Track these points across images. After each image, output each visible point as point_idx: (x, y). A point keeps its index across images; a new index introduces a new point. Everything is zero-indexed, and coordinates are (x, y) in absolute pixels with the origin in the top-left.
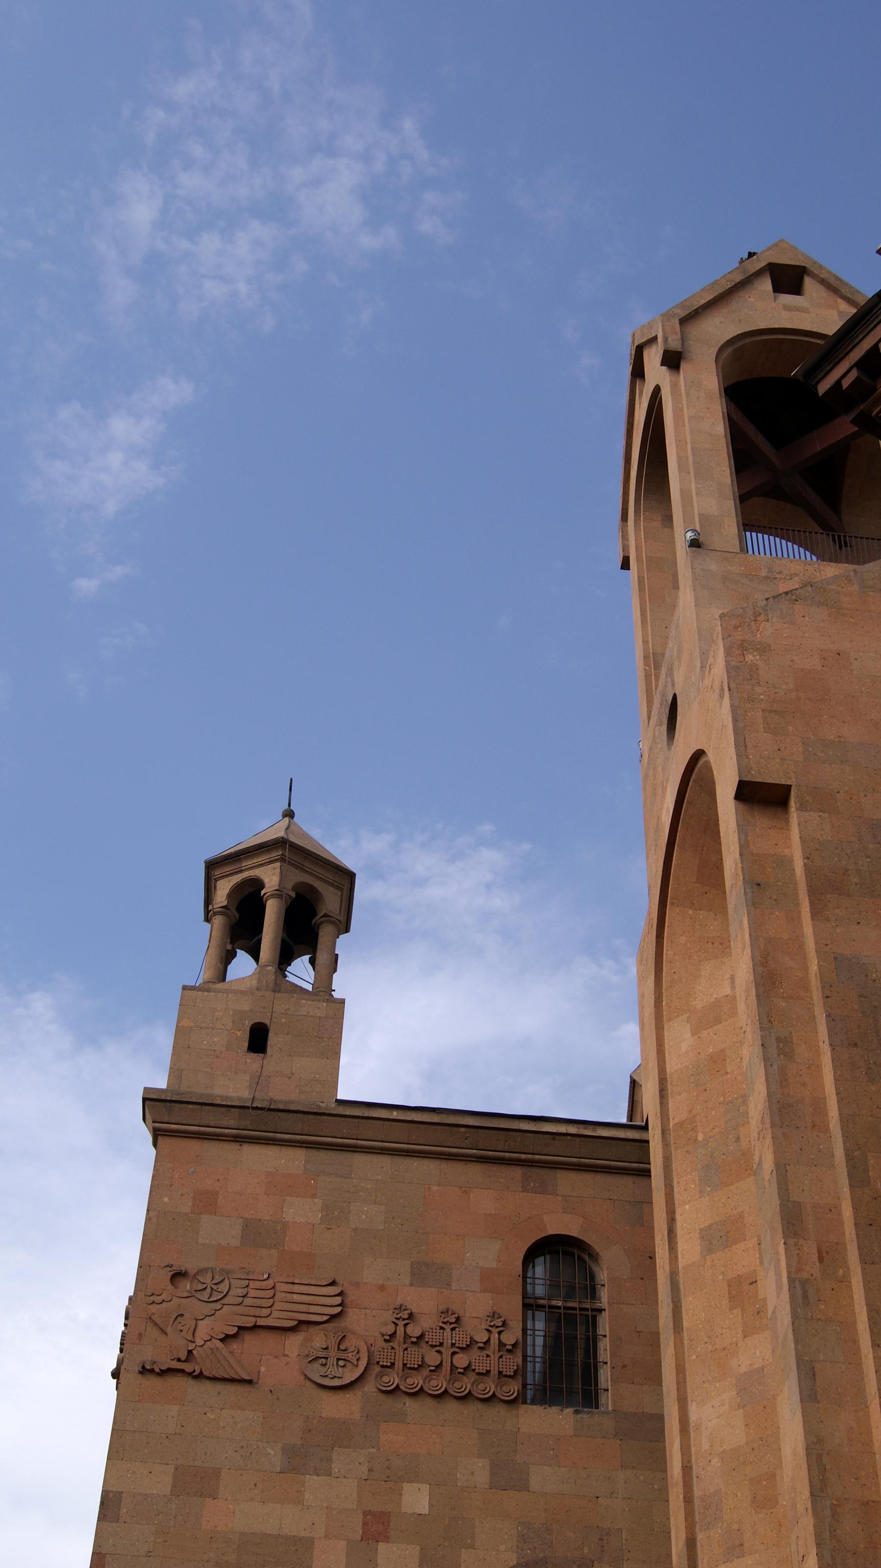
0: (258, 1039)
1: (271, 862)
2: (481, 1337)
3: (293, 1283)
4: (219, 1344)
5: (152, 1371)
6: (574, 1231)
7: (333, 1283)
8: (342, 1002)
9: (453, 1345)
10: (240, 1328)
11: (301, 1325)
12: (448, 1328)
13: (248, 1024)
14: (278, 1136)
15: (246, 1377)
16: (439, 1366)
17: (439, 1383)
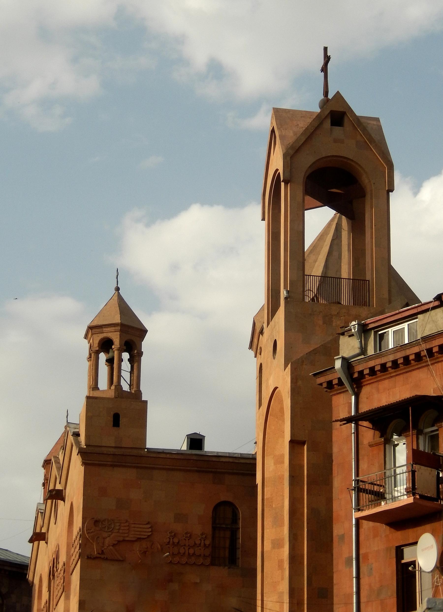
0: (116, 420)
1: (115, 331)
2: (198, 542)
3: (135, 524)
4: (111, 547)
5: (91, 558)
6: (230, 500)
7: (148, 523)
8: (146, 402)
9: (189, 545)
10: (119, 541)
11: (139, 539)
12: (187, 539)
13: (112, 413)
14: (127, 464)
15: (122, 559)
16: (184, 553)
17: (184, 560)
